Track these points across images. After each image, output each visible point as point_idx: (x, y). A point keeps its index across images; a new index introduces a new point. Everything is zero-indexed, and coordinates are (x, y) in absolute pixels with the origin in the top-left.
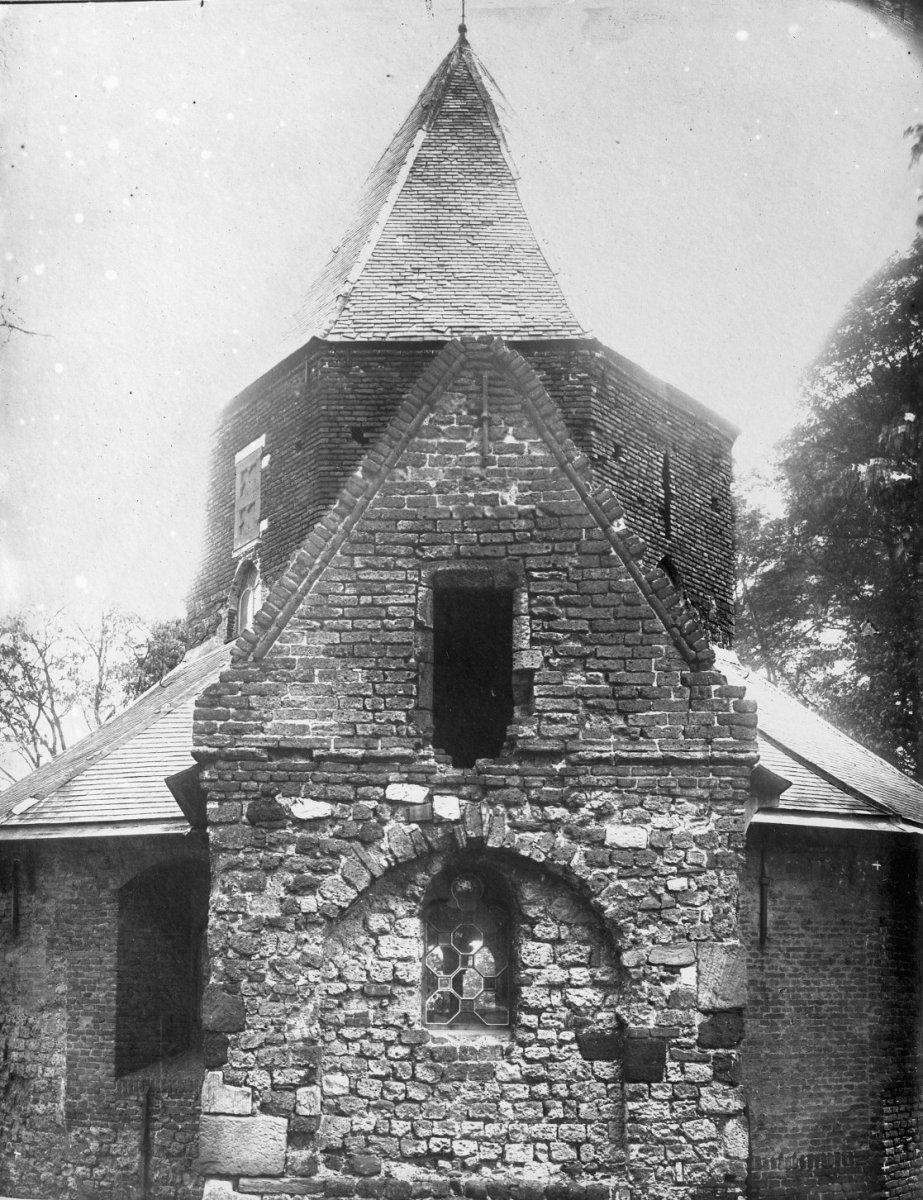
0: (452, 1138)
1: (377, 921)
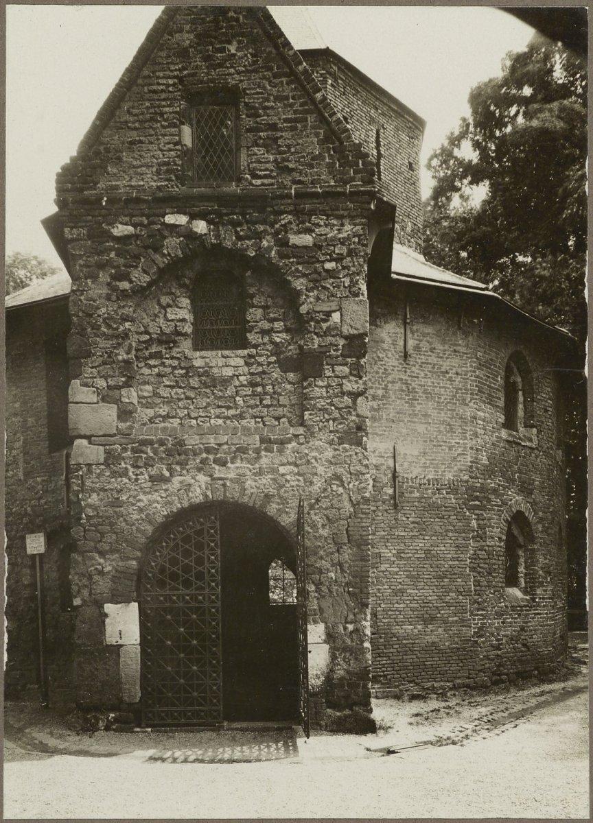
0: (210, 417)
1: (165, 300)
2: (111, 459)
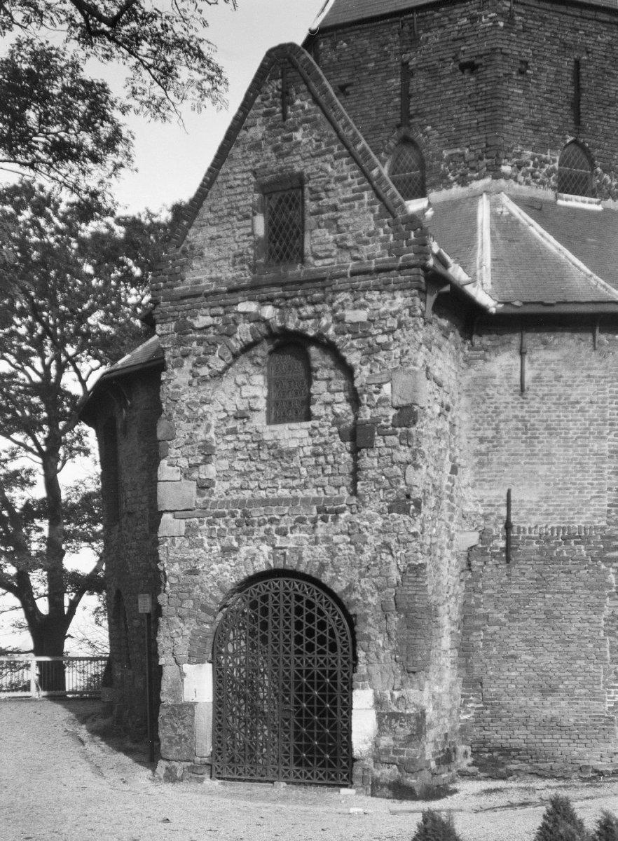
2: (191, 531)
